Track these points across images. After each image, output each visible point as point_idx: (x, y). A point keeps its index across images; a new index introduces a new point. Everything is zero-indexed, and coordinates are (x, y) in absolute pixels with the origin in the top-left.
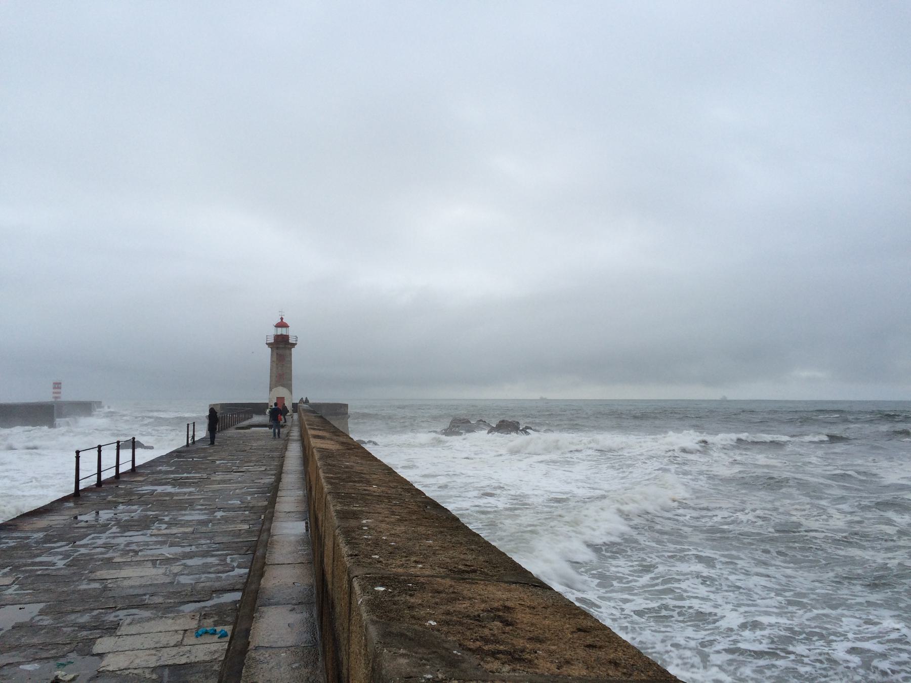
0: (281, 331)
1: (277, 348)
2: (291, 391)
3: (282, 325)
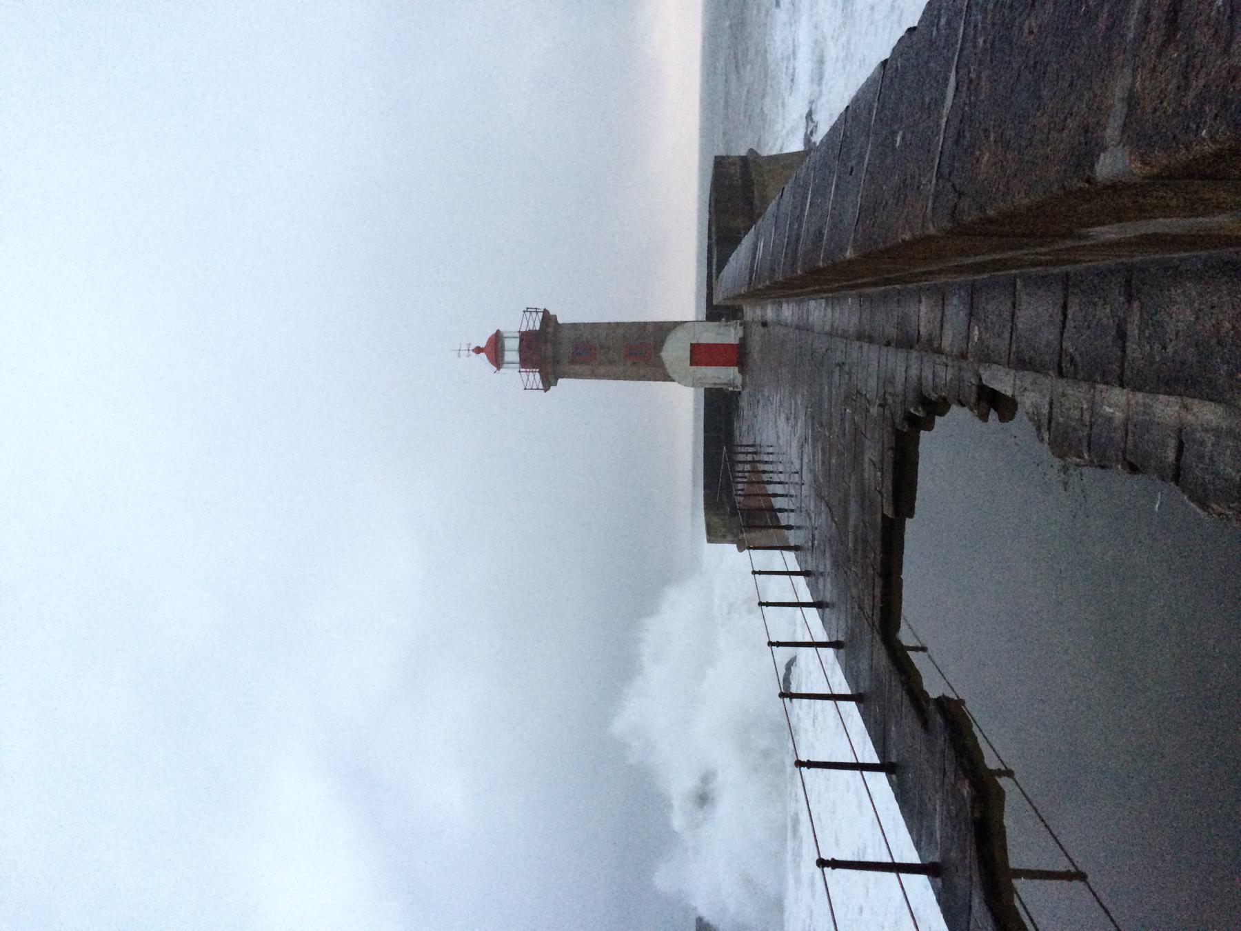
0: (512, 353)
1: (556, 361)
2: (676, 325)
3: (494, 350)
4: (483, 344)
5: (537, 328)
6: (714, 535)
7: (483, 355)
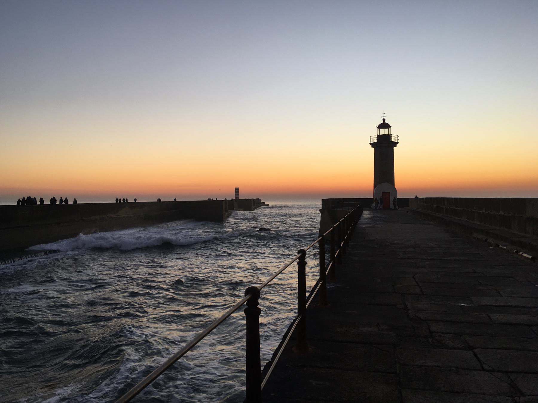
3: (384, 125)
4: (386, 122)
5: (393, 140)
6: (323, 201)
7: (382, 122)
